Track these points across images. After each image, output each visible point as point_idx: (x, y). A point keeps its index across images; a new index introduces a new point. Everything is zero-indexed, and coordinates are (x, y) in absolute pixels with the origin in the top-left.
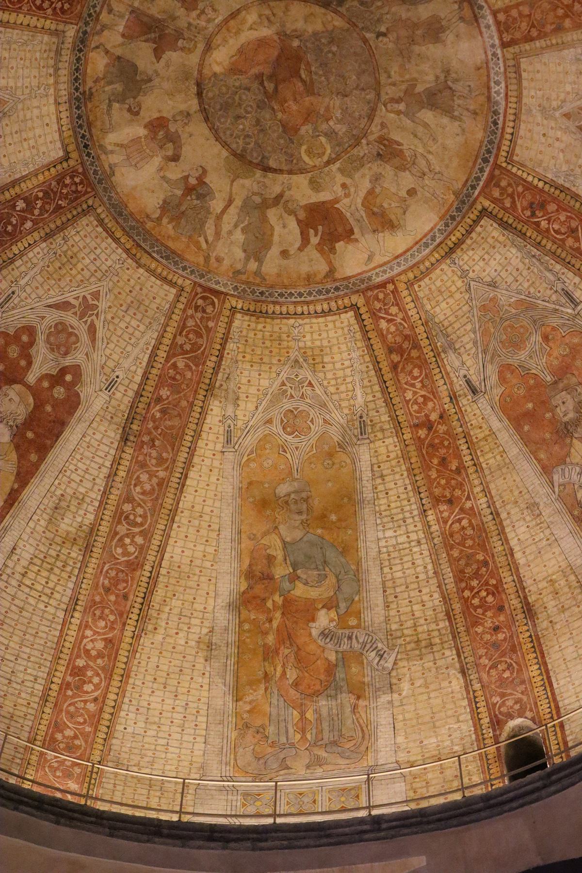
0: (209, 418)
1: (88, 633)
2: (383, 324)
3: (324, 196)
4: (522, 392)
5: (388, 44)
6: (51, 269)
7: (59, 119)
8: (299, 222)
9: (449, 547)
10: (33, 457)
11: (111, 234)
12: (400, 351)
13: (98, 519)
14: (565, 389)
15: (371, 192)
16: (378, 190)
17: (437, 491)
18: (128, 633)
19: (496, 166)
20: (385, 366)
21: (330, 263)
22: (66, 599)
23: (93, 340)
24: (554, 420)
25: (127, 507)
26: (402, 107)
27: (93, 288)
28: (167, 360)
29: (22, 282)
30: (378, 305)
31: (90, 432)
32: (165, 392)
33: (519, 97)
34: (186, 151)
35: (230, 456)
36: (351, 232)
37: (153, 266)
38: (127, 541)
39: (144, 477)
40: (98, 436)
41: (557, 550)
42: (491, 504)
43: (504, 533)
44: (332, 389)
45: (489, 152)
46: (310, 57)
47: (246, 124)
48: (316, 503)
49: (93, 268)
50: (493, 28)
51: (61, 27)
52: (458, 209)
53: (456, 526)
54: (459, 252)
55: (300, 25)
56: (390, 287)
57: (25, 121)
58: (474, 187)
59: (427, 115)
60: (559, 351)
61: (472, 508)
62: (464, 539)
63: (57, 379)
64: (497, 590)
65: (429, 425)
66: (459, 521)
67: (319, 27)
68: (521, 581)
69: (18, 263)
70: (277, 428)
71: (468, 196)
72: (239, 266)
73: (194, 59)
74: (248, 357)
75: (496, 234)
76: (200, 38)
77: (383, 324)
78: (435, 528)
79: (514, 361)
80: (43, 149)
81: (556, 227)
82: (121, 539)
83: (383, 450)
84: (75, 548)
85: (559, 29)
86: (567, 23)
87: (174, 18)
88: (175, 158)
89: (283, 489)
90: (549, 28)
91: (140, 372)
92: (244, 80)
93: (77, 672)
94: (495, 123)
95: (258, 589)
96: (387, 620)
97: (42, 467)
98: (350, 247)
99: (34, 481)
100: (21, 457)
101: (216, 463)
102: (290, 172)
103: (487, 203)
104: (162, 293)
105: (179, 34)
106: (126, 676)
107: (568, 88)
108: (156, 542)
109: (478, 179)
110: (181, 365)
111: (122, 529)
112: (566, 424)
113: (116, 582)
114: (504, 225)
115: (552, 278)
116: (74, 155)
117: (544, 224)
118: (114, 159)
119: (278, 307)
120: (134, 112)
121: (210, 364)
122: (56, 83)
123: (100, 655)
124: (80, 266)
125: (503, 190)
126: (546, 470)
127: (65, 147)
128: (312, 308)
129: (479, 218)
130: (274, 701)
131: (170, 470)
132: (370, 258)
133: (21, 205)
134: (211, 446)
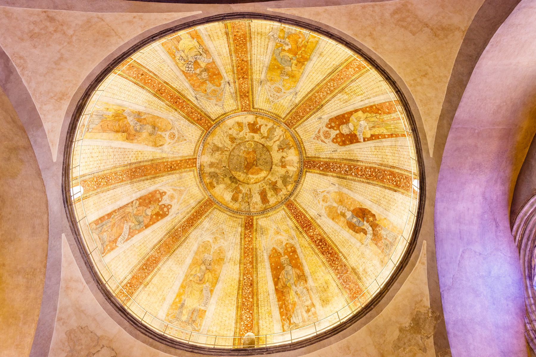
0: (300, 100)
1: (352, 73)
2: (248, 102)
3: (252, 134)
4: (216, 80)
5: (224, 164)
6: (322, 151)
7: (304, 181)
8: (260, 131)
9: (246, 51)
10: (346, 116)
11: (305, 149)
12: (245, 96)
13: (337, 93)
14: (203, 79)
15: (240, 131)
16: (238, 131)
17: (246, 63)
18: (341, 68)
19: (207, 131)
20: (250, 93)
21: (256, 119)
22: (354, 83)
23: (320, 130)
24: (209, 72)
25: (329, 92)
26: (226, 149)
27: (314, 141)
28: (304, 116)
29: (329, 152)
30: (248, 107)
31: (330, 112)
32: (308, 110)
33: (196, 146)
34: (280, 158)
35: (298, 90)
36: (248, 124)
37: (298, 137)
38: (332, 86)
39: (321, 96)
40: (328, 110)
41: (215, 45)
42: (231, 58)
43: (230, 51)
44: (266, 93)
45: (208, 134)
46: (243, 166)
47: (264, 157)
48: (279, 71)
49: (312, 145)
50: (197, 163)
51: (293, 201)
52: (220, 122)
53: (243, 55)
54: (223, 113)
55: (242, 175)
56: (243, 110)
57: (311, 186)
58: (214, 127)
59: (220, 146)
60: (204, 87)
61: (237, 58)
62: (241, 52)
63: (332, 127)
64: (235, 40)
65: (243, 78)
66: (241, 56)
67: (238, 173)
68: (228, 40)
69: (328, 157)
70: (283, 91)
71: (216, 125)
72: (278, 127)
73: (269, 177)
74: (284, 108)
75: (212, 115)
76: (266, 181)
77: (248, 102)
78: (249, 56)
79: (216, 87)
80: (311, 177)
81: (196, 115)
82: (333, 87)
83: (257, 76)
84: (346, 91)
85: (181, 161)
86: (179, 162)
87: (269, 188)
88: (283, 157)
89: (287, 78)
90: (184, 161)
91: (312, 117)
92: (260, 167)
93: (360, 69)
94: (204, 140)
95: (302, 60)
96: (269, 42)
97: (345, 112)
98: (250, 121)
99: (349, 111)
100: (349, 118)
101: (302, 90)
102: (258, 142)
103: (212, 122)
104: (299, 130)
105: (270, 184)
106: (346, 60)
107: (183, 146)
108: (325, 82)
109: (213, 128)
110: (301, 114)
111: (332, 88)
112: (205, 71)
113: (339, 79)
114: (209, 117)
115: (200, 103)
116: (304, 171)
117: (199, 115)
118: (296, 165)
119: (273, 115)
120: (287, 172)
121: (294, 110)
122: (301, 189)
123: (351, 68)
124: (315, 147)
125: (207, 125)
126: (214, 62)
127: (306, 174)
128: (264, 112)
129: (215, 120)
130: (307, 37)
131: (314, 94)
132: (246, 117)
133: (321, 168)
134: (301, 94)
